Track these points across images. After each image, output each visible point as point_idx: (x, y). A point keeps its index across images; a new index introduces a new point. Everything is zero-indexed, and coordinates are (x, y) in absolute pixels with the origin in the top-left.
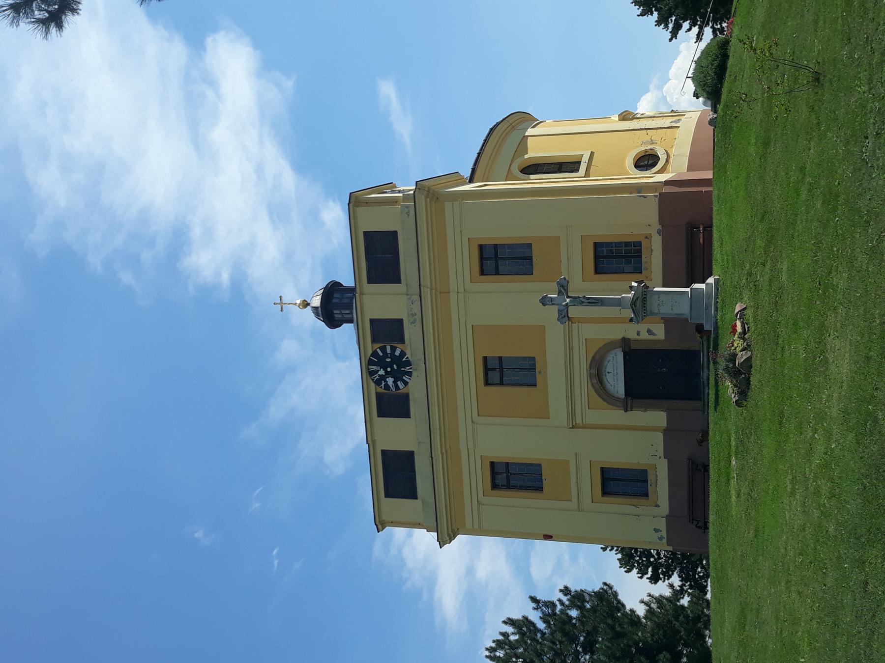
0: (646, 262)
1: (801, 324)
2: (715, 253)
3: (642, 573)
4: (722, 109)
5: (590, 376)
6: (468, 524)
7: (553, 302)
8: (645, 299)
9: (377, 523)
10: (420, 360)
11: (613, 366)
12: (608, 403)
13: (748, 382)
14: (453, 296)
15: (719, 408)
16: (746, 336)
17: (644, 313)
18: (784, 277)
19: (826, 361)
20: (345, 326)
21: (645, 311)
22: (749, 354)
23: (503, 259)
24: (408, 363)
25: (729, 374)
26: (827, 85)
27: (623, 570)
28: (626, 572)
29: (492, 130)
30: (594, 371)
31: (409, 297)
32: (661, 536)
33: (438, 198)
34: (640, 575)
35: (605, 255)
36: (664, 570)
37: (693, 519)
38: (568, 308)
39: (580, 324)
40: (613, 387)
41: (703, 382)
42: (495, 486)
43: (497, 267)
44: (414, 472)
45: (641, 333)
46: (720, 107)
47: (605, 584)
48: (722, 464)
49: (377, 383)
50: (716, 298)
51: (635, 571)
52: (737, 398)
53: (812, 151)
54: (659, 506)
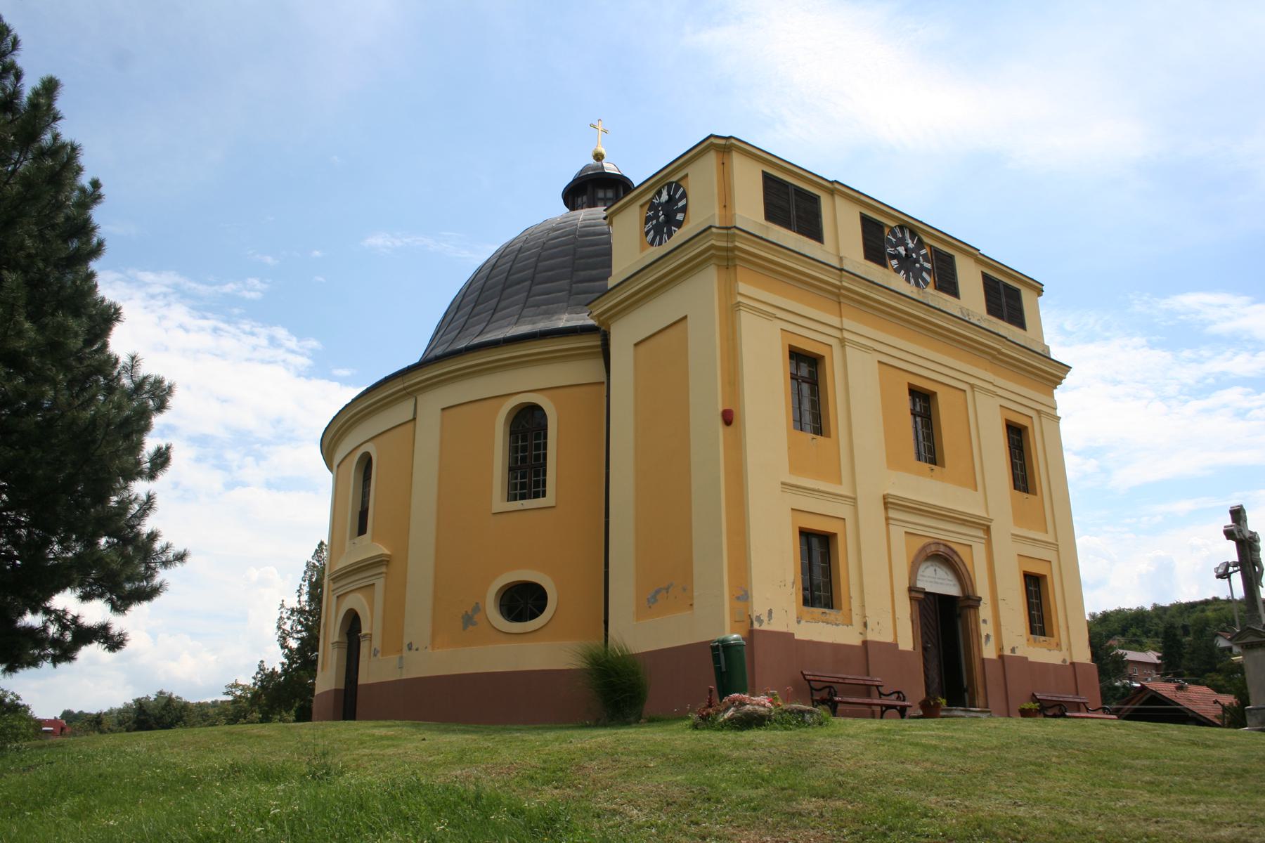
5: (938, 543)
11: (943, 579)
41: (952, 710)
49: (892, 231)
54: (799, 622)
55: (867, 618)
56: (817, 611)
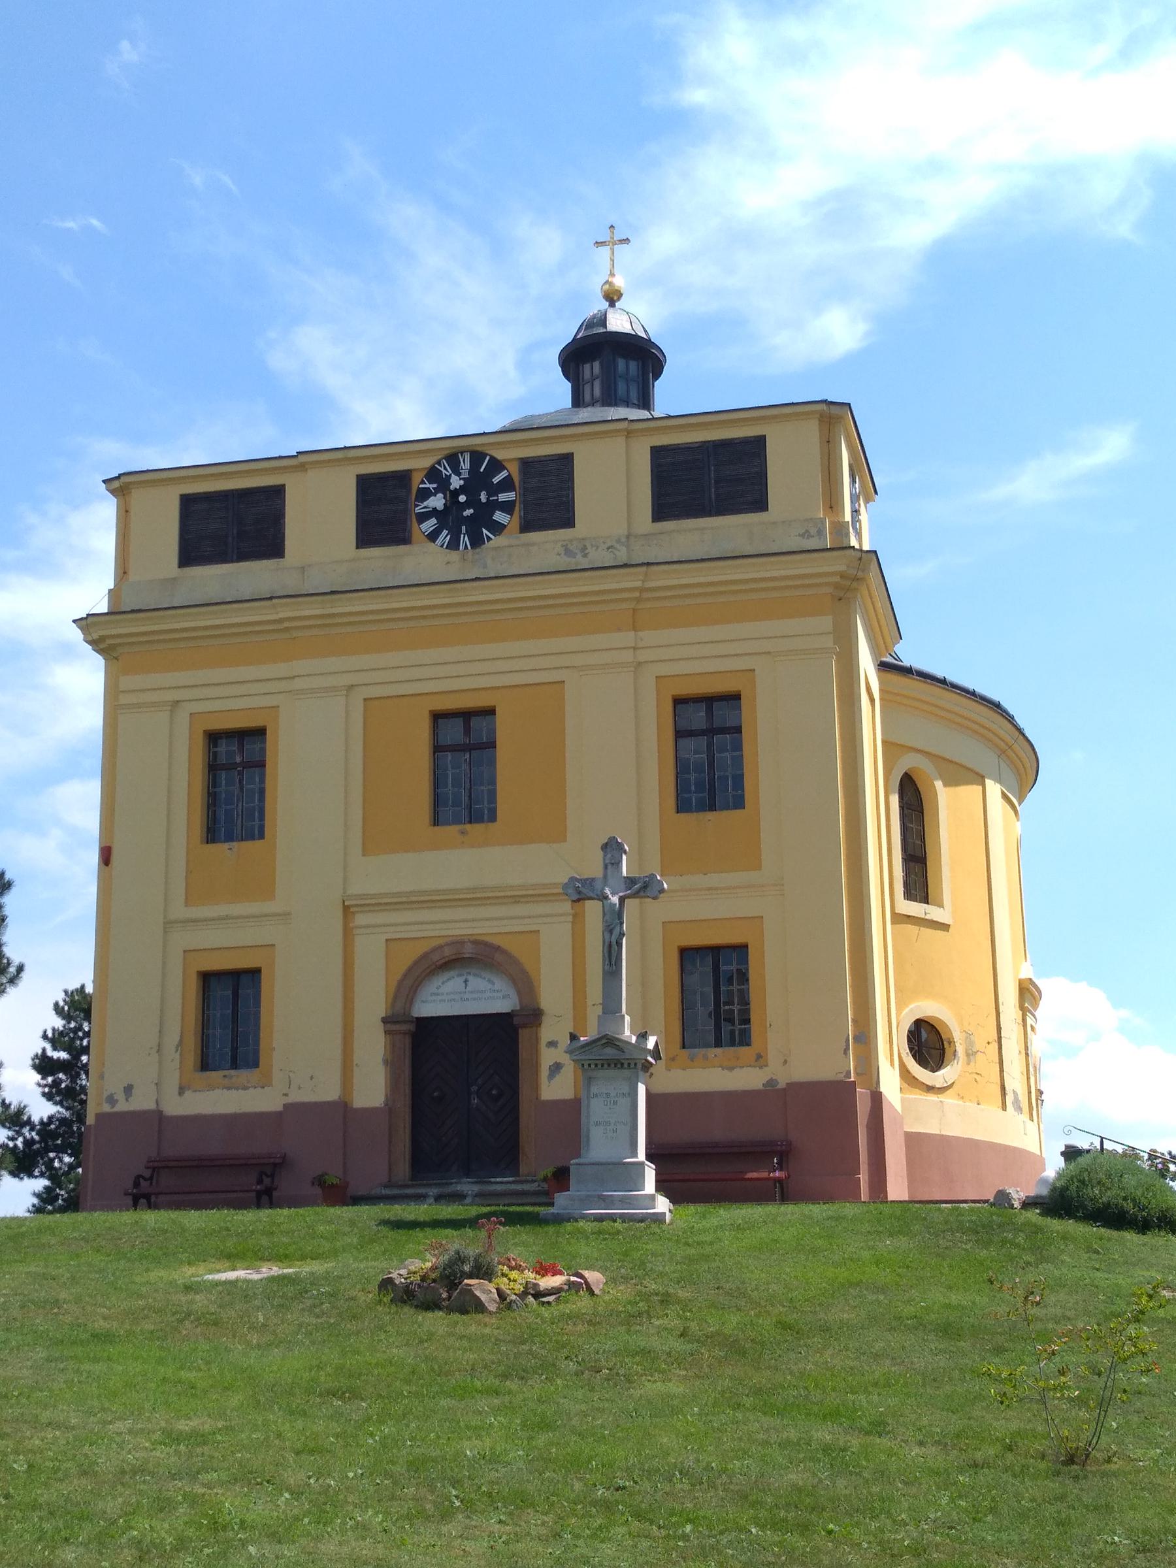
0: (706, 1058)
1: (541, 1439)
2: (722, 1212)
3: (56, 1039)
4: (1028, 1223)
5: (458, 942)
6: (126, 682)
7: (609, 867)
8: (619, 1066)
9: (123, 479)
10: (485, 567)
12: (400, 983)
13: (431, 1305)
14: (628, 638)
15: (385, 1230)
16: (531, 1299)
17: (589, 1065)
18: (653, 1387)
19: (446, 1515)
20: (564, 388)
21: (593, 1066)
22: (492, 1307)
23: (710, 745)
24: (477, 541)
25: (451, 1264)
26: (1054, 1486)
27: (60, 997)
28: (56, 1005)
29: (996, 706)
30: (468, 951)
31: (623, 540)
32: (117, 1101)
33: (840, 599)
34: (50, 1034)
35: (722, 968)
36: (63, 1086)
37: (154, 1169)
38: (599, 900)
39: (570, 918)
40: (436, 991)
41: (452, 1184)
42: (213, 738)
43: (691, 733)
44: (242, 557)
45: (552, 1049)
46: (1033, 1215)
47: (20, 969)
48: (265, 1241)
49: (433, 474)
50: (624, 1218)
51: (59, 1023)
52: (397, 1282)
53: (916, 1450)
55: (291, 1074)
56: (215, 1076)
